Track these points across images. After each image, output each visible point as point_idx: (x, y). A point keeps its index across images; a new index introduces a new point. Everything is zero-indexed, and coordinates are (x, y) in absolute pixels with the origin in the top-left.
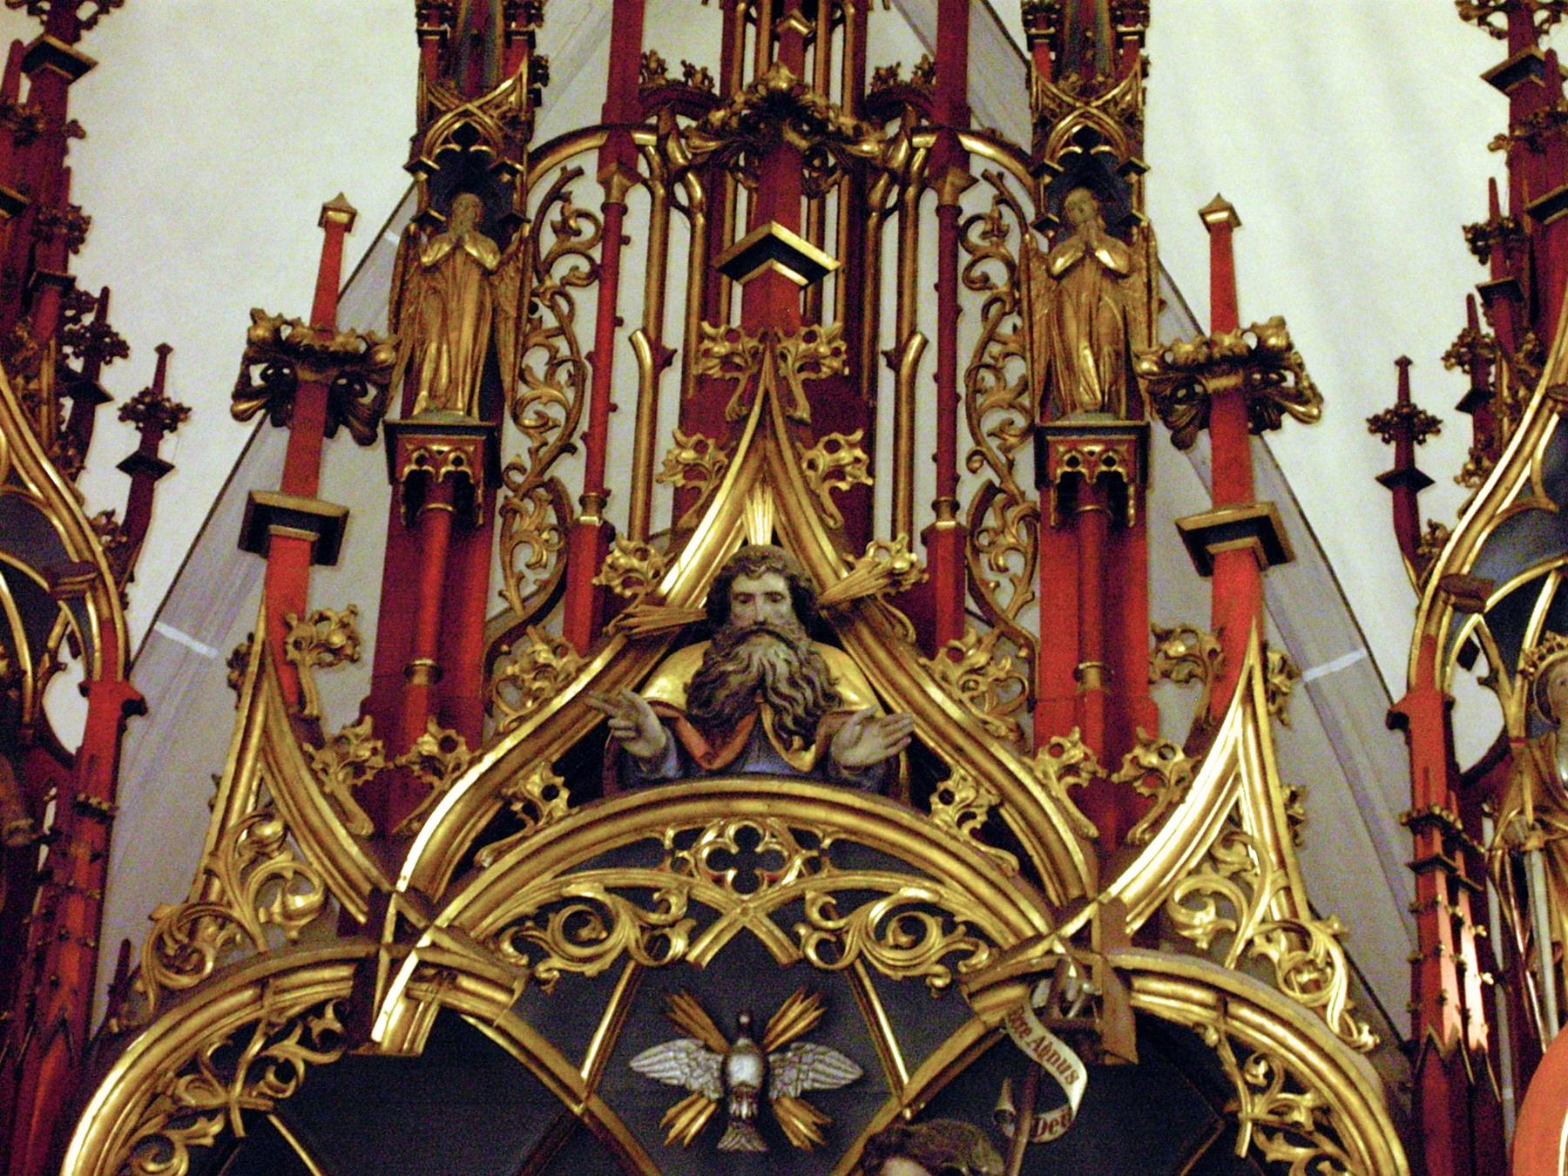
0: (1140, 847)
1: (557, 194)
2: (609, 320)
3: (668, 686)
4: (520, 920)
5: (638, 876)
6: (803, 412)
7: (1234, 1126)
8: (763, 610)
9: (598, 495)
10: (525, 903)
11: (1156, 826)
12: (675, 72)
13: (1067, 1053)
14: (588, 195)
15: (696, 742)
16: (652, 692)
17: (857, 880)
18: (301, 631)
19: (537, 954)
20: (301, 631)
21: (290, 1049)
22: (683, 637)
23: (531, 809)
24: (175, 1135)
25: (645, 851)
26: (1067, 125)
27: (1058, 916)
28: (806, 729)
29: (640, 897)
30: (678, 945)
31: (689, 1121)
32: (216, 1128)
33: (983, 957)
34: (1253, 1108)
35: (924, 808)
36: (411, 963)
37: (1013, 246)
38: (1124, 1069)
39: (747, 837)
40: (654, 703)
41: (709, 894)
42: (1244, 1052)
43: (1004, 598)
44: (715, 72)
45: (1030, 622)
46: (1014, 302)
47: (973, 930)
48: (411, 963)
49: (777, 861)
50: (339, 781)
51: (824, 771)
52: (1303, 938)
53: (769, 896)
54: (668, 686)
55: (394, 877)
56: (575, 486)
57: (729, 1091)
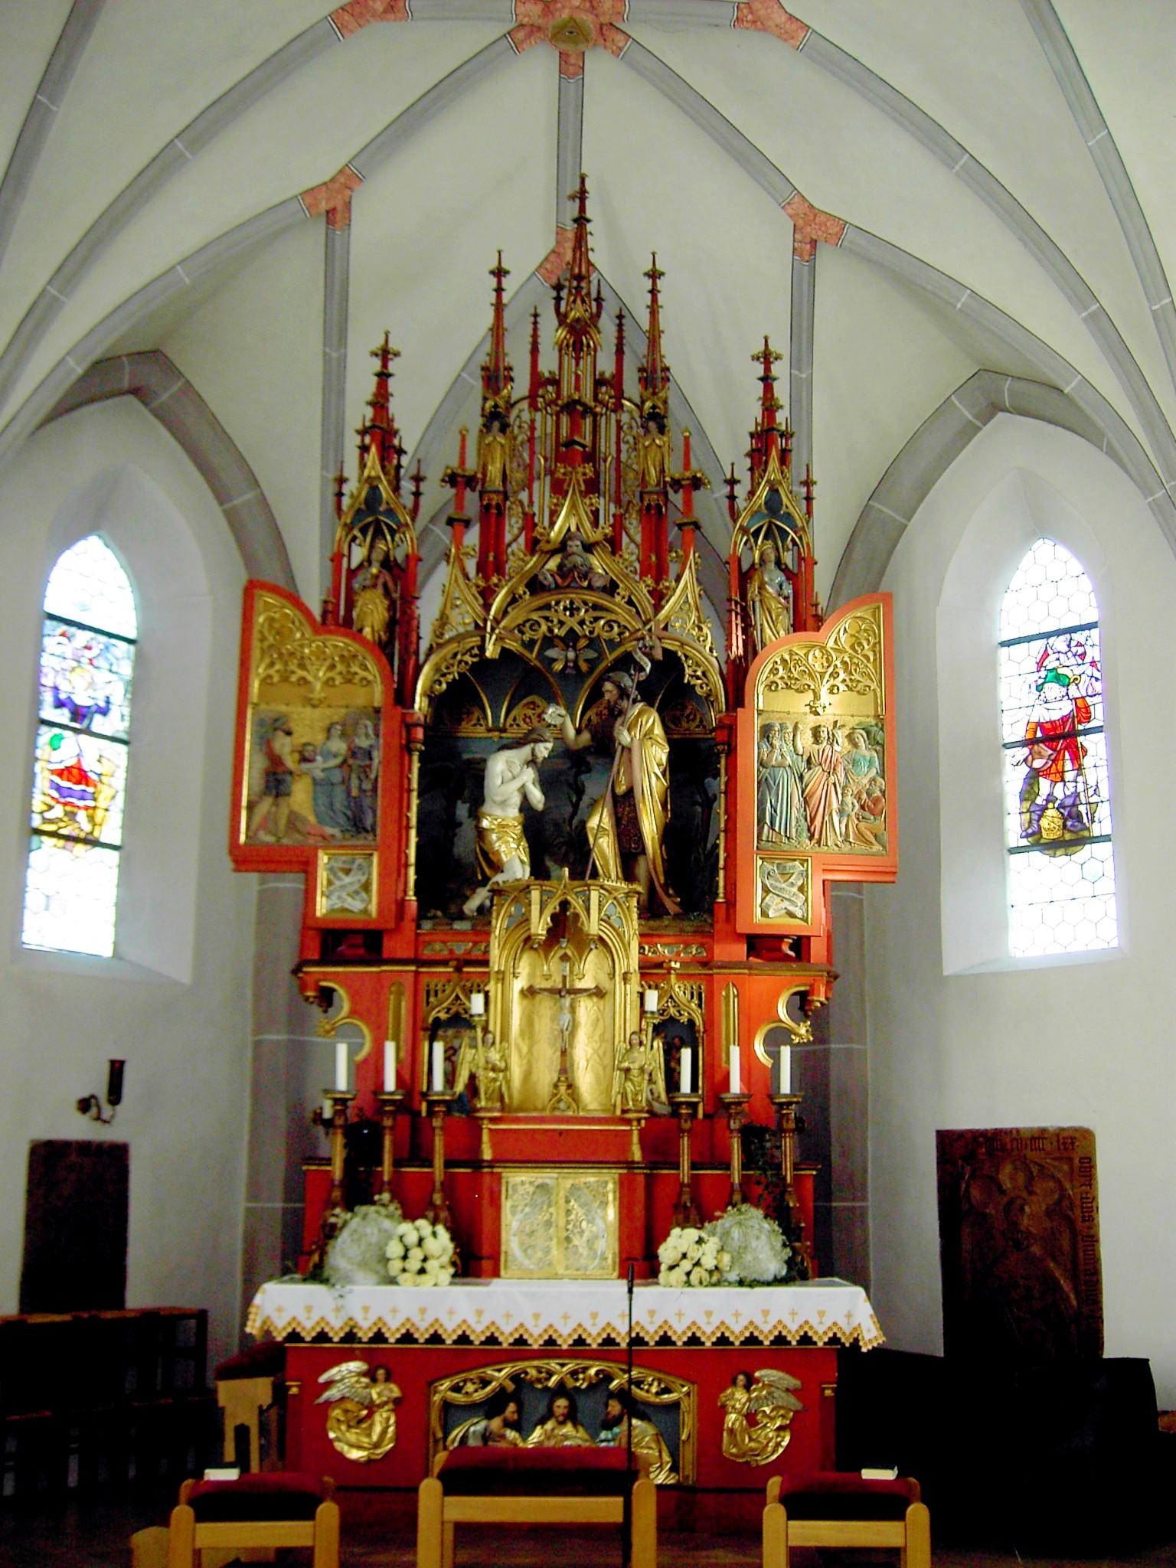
0: (663, 607)
1: (518, 416)
3: (553, 564)
4: (519, 625)
5: (546, 613)
6: (583, 488)
7: (684, 675)
8: (575, 549)
9: (531, 503)
10: (520, 621)
11: (668, 601)
12: (547, 375)
13: (646, 660)
14: (526, 416)
15: (559, 580)
16: (547, 567)
17: (598, 614)
18: (462, 551)
19: (523, 633)
20: (462, 551)
21: (468, 658)
22: (553, 553)
23: (520, 597)
24: (442, 679)
25: (548, 607)
26: (648, 404)
27: (645, 624)
28: (585, 576)
29: (547, 619)
30: (556, 631)
31: (558, 666)
32: (451, 677)
33: (627, 634)
34: (688, 671)
35: (613, 596)
36: (494, 637)
37: (634, 432)
38: (659, 661)
39: (572, 603)
40: (548, 570)
41: (563, 618)
42: (686, 657)
43: (632, 532)
44: (557, 373)
45: (638, 538)
47: (625, 627)
48: (494, 637)
49: (578, 609)
50: (474, 590)
51: (590, 587)
52: (700, 629)
53: (577, 618)
55: (488, 614)
56: (526, 502)
57: (567, 661)
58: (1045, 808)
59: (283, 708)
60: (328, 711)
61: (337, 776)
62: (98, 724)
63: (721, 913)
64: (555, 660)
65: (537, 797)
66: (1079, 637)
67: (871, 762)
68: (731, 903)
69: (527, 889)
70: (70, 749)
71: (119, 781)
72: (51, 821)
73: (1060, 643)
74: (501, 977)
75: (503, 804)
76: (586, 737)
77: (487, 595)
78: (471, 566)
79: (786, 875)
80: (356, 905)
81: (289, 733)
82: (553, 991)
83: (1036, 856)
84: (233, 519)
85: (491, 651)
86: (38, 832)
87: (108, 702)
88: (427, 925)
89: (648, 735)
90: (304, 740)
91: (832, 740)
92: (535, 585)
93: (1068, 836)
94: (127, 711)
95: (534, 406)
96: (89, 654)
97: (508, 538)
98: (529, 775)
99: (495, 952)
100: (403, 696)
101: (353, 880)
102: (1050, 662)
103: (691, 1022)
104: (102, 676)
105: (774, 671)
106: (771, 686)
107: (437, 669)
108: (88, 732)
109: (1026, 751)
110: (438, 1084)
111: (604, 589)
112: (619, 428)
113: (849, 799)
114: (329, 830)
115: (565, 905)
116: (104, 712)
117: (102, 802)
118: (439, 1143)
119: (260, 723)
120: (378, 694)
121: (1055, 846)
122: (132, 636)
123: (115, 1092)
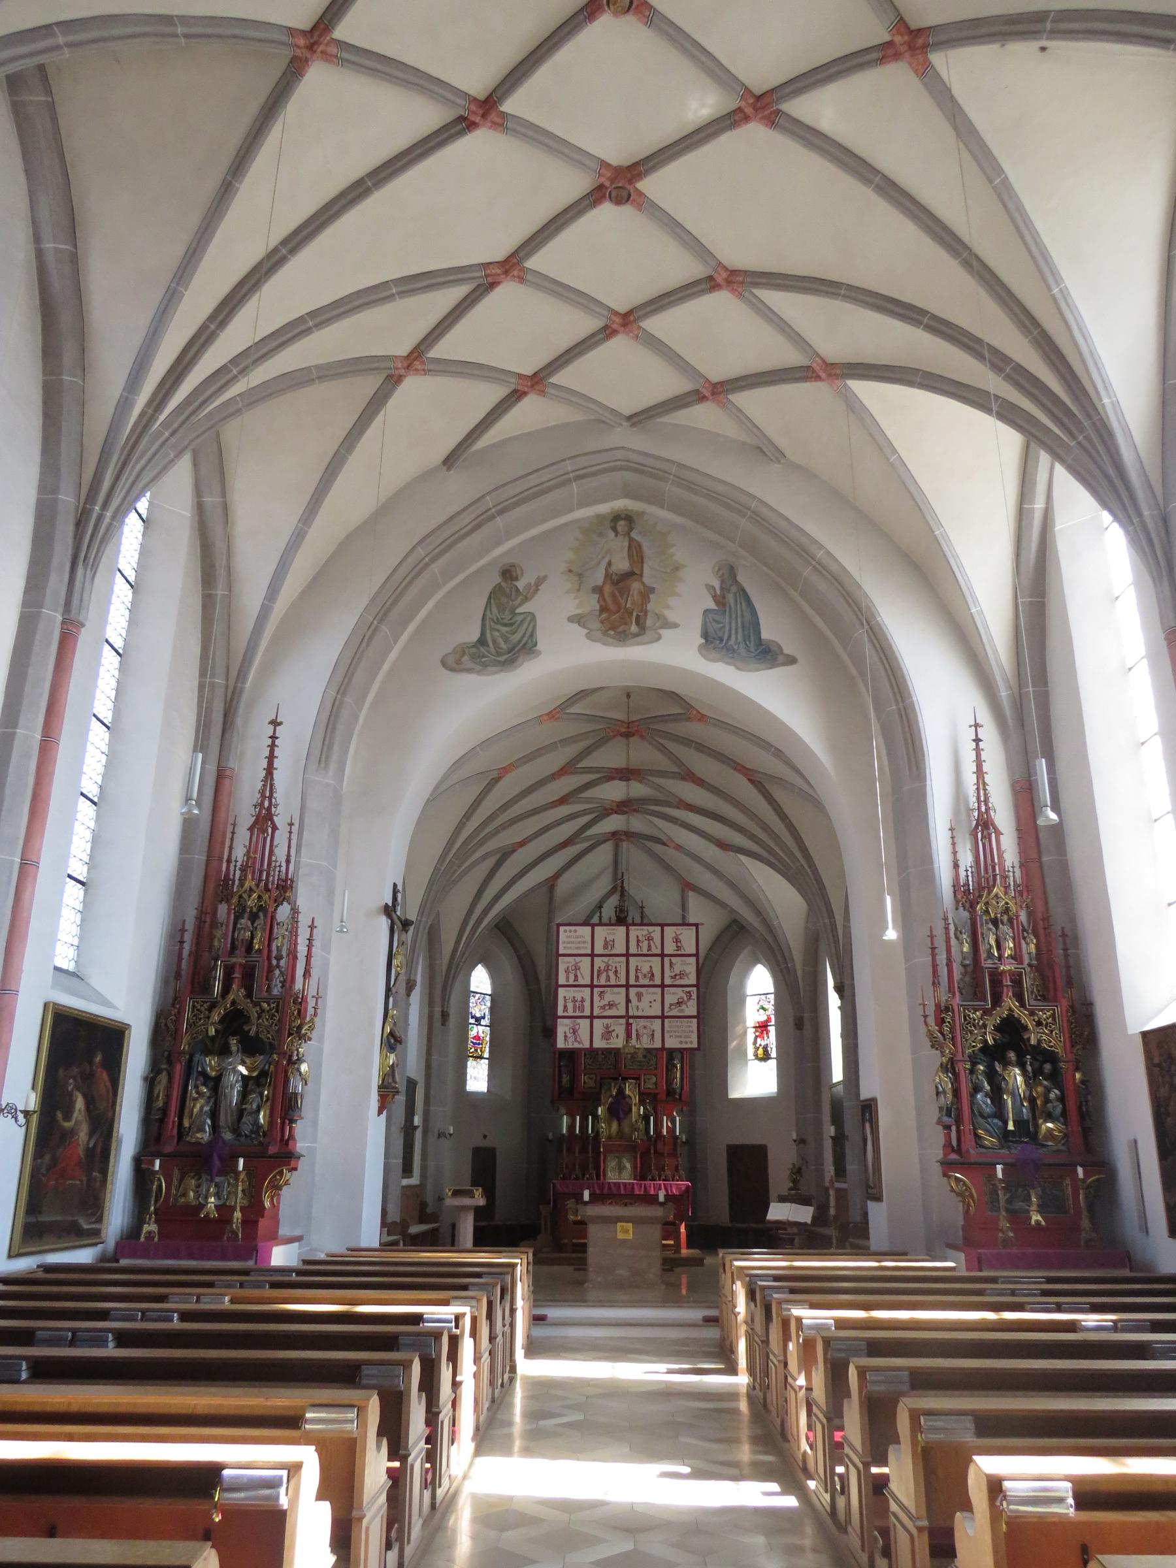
66: (768, 996)
71: (488, 1039)
73: (763, 997)
84: (520, 958)
102: (761, 1003)
104: (483, 1007)
122: (490, 993)
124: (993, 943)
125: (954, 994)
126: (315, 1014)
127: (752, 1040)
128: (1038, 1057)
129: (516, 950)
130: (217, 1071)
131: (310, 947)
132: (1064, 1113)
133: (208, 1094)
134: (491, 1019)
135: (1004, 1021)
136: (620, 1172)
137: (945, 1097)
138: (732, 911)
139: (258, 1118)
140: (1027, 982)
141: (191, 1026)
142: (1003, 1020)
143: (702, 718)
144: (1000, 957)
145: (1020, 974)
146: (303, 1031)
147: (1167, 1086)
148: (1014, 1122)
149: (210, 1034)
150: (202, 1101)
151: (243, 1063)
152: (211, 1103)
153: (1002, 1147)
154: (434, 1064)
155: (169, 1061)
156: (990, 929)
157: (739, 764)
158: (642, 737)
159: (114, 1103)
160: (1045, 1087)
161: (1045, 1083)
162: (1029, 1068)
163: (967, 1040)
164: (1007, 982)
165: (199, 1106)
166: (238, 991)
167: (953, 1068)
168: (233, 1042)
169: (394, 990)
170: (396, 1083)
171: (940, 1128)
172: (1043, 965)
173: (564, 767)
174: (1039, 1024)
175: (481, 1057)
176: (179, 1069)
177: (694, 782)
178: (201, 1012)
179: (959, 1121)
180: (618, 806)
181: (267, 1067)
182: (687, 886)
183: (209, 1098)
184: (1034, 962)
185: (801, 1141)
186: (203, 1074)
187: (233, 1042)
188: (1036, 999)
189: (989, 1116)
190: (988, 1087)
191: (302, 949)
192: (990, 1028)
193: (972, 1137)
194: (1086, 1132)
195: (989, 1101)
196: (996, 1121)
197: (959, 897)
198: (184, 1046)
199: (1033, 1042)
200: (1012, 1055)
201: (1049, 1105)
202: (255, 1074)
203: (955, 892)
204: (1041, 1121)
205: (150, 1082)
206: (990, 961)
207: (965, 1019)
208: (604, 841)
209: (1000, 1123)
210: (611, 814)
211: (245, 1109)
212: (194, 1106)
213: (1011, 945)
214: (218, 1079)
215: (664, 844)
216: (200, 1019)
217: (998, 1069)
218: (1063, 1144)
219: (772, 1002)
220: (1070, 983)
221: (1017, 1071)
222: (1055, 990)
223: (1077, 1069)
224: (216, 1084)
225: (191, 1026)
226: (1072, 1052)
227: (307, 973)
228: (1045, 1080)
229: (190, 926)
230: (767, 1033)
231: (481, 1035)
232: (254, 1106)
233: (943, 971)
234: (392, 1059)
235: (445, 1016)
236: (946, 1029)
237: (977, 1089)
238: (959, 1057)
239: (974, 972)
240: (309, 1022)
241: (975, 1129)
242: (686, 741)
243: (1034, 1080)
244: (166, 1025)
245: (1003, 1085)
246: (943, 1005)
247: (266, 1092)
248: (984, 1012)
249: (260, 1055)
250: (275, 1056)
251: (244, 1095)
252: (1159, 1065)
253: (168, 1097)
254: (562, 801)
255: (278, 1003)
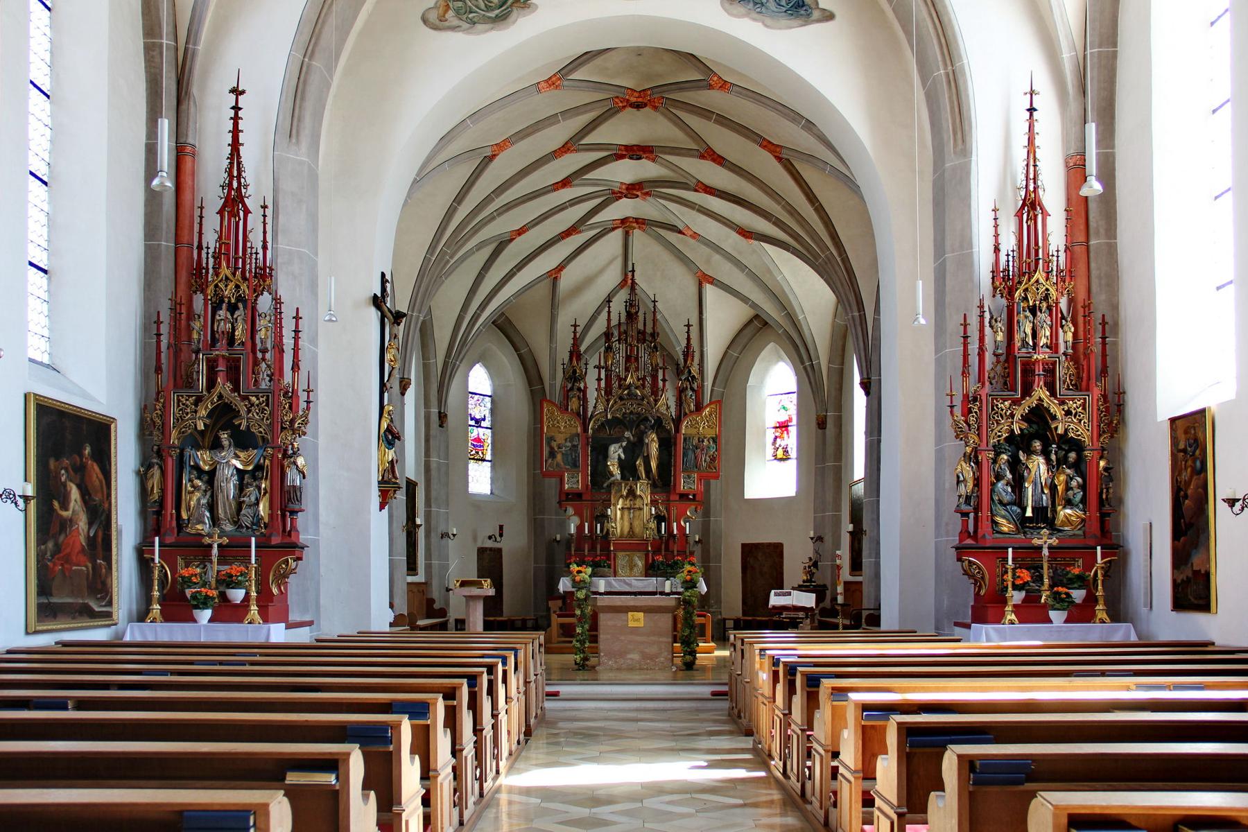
2: (619, 357)
3: (626, 392)
14: (617, 346)
22: (627, 389)
25: (624, 404)
46: (649, 355)
54: (626, 392)
58: (778, 448)
59: (553, 434)
60: (564, 435)
61: (569, 452)
62: (483, 424)
63: (672, 487)
64: (626, 417)
65: (623, 456)
67: (713, 448)
68: (675, 485)
69: (620, 484)
70: (474, 433)
71: (489, 441)
72: (472, 455)
74: (615, 505)
75: (614, 459)
76: (636, 439)
77: (608, 401)
78: (603, 392)
79: (689, 477)
80: (575, 486)
81: (555, 441)
82: (627, 508)
83: (775, 461)
84: (521, 357)
85: (609, 417)
86: (470, 459)
87: (485, 416)
88: (594, 491)
89: (653, 440)
90: (560, 442)
91: (703, 441)
92: (621, 398)
93: (784, 457)
94: (490, 419)
95: (619, 343)
96: (479, 402)
97: (613, 382)
98: (621, 450)
99: (612, 499)
100: (585, 430)
101: (575, 480)
102: (781, 404)
103: (664, 516)
104: (483, 408)
105: (688, 423)
106: (686, 427)
107: (594, 422)
108: (480, 426)
109: (774, 430)
110: (598, 532)
111: (641, 399)
112: (645, 349)
113: (708, 458)
114: (567, 467)
115: (631, 487)
116: (484, 419)
117: (485, 448)
118: (599, 546)
119: (548, 438)
120: (579, 430)
121: (781, 460)
122: (490, 394)
123: (501, 535)
124: (1029, 331)
125: (983, 384)
126: (308, 408)
127: (772, 440)
128: (1063, 446)
129: (516, 349)
130: (210, 465)
131: (296, 339)
132: (1083, 501)
133: (203, 487)
134: (492, 421)
135: (1032, 411)
136: (631, 569)
137: (966, 486)
138: (754, 305)
139: (257, 511)
140: (1060, 372)
141: (178, 420)
142: (1032, 410)
143: (724, 85)
144: (1035, 346)
145: (1054, 364)
146: (296, 425)
147: (1189, 470)
148: (1033, 509)
149: (199, 428)
150: (198, 494)
151: (237, 457)
152: (208, 497)
153: (1019, 533)
154: (433, 466)
155: (159, 454)
156: (1026, 317)
157: (764, 139)
158: (655, 108)
159: (109, 495)
160: (1068, 475)
161: (1068, 471)
162: (1053, 457)
163: (992, 431)
164: (1039, 370)
165: (196, 498)
166: (224, 385)
167: (976, 457)
168: (224, 436)
169: (388, 385)
170: (396, 478)
171: (959, 515)
172: (1077, 356)
173: (566, 143)
174: (1068, 413)
175: (483, 460)
176: (171, 464)
177: (714, 160)
178: (187, 406)
179: (977, 510)
180: (627, 189)
181: (262, 461)
182: (703, 279)
183: (205, 491)
184: (1070, 351)
185: (819, 539)
186: (197, 468)
187: (224, 436)
188: (1068, 389)
189: (1009, 504)
190: (1009, 476)
191: (288, 342)
192: (1018, 416)
193: (989, 523)
194: (1103, 517)
195: (1009, 489)
196: (1015, 508)
197: (998, 283)
198: (174, 439)
199: (1060, 431)
200: (1037, 445)
201: (1070, 493)
202: (250, 468)
203: (993, 278)
204: (1059, 508)
205: (143, 477)
206: (1024, 350)
207: (993, 409)
208: (613, 229)
209: (1019, 510)
210: (620, 198)
211: (244, 502)
212: (190, 499)
213: (1048, 333)
214: (212, 474)
215: (680, 232)
216: (187, 414)
217: (1022, 458)
218: (1079, 529)
219: (795, 402)
220: (1104, 371)
221: (1041, 460)
222: (1089, 379)
223: (1101, 458)
224: (210, 477)
225: (178, 420)
226: (1098, 441)
227: (296, 367)
228: (1069, 468)
229: (165, 317)
230: (788, 433)
231: (481, 436)
232: (253, 499)
233: (974, 360)
234: (391, 454)
235: (442, 417)
236: (972, 420)
237: (999, 477)
238: (983, 447)
239: (1007, 361)
240: (301, 417)
241: (993, 515)
242: (705, 113)
243: (1058, 469)
244: (152, 419)
245: (1026, 474)
246: (971, 395)
247: (263, 486)
248: (1012, 402)
249: (254, 449)
250: (270, 451)
251: (241, 488)
252: (1184, 451)
253: (163, 490)
254: (565, 183)
255: (268, 396)
